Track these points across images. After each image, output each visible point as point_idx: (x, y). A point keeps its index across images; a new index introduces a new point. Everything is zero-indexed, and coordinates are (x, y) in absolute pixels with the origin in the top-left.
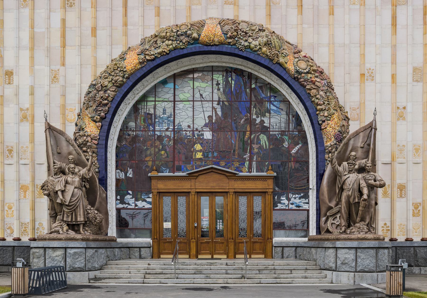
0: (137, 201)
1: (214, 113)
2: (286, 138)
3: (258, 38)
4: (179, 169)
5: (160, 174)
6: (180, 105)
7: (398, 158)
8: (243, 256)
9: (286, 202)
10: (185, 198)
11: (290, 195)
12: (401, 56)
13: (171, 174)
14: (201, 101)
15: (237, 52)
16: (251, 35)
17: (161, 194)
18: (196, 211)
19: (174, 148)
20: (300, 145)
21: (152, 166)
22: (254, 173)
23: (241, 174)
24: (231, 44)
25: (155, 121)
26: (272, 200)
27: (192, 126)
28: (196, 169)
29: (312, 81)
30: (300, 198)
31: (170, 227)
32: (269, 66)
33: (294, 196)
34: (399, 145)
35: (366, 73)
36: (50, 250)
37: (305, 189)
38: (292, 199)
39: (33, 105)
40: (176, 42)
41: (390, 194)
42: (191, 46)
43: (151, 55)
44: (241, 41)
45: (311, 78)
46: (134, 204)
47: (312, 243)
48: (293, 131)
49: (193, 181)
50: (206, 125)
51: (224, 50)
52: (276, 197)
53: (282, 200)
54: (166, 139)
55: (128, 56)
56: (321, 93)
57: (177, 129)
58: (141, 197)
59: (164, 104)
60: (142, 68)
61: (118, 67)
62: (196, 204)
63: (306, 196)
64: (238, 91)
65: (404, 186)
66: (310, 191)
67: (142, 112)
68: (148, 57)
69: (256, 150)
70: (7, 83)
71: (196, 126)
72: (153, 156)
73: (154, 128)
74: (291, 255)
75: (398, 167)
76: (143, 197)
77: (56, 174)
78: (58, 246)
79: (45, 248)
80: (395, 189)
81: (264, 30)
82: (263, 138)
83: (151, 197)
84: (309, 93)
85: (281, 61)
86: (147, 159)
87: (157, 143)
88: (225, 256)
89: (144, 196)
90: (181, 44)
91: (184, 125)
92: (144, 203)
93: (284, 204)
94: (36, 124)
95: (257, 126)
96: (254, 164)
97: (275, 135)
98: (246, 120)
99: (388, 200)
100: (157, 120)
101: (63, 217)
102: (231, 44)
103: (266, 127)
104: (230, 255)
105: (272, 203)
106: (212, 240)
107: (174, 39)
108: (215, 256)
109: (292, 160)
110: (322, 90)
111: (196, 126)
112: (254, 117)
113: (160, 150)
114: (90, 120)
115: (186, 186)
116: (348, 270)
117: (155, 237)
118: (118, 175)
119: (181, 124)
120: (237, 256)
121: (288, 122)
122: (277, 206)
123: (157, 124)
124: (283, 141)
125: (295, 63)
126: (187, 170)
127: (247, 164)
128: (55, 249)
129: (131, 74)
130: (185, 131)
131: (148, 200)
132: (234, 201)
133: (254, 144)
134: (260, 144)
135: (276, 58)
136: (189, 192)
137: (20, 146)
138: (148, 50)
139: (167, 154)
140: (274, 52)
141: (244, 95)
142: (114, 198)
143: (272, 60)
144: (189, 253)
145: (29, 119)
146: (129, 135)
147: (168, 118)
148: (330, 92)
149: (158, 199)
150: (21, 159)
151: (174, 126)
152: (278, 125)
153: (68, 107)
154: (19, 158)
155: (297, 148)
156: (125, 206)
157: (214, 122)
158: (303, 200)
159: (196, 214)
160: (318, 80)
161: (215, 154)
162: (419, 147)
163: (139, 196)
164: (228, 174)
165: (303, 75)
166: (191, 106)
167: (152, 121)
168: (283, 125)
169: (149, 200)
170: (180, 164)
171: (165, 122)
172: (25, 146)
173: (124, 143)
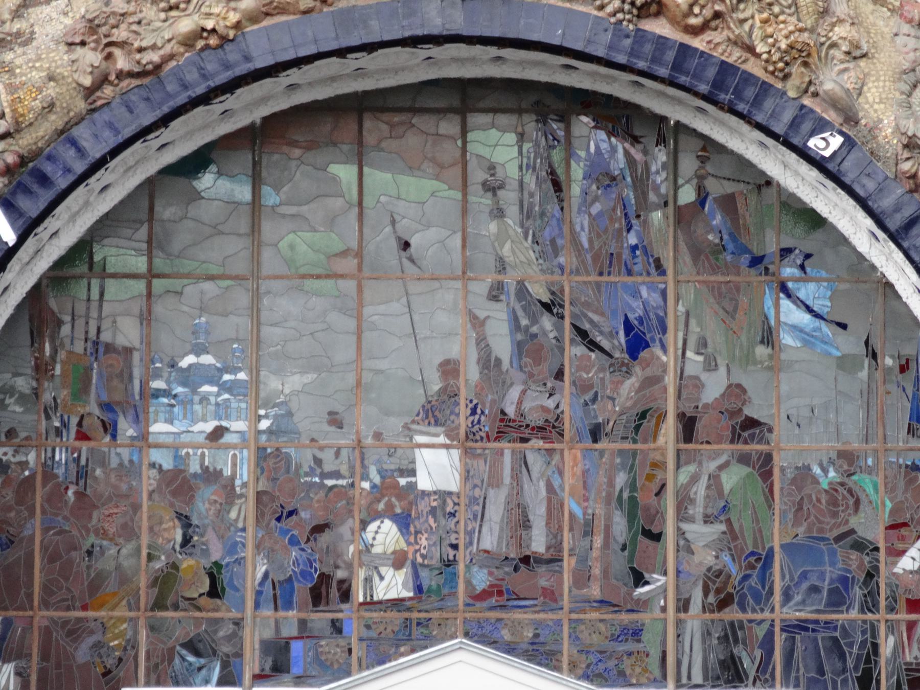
57: (269, 431)
171: (204, 399)
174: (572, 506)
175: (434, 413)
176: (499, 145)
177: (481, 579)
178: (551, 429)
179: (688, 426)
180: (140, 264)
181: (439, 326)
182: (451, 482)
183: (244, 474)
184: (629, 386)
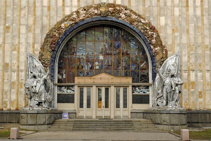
9: (138, 90)
20: (145, 63)
30: (145, 89)
35: (175, 29)
38: (141, 89)
46: (66, 91)
57: (87, 54)
74: (141, 117)
93: (138, 91)
155: (143, 64)
158: (146, 89)
174: (113, 61)
175: (101, 53)
176: (107, 30)
177: (105, 67)
178: (111, 54)
179: (123, 54)
180: (76, 40)
181: (101, 46)
182: (103, 59)
183: (85, 58)
184: (118, 51)
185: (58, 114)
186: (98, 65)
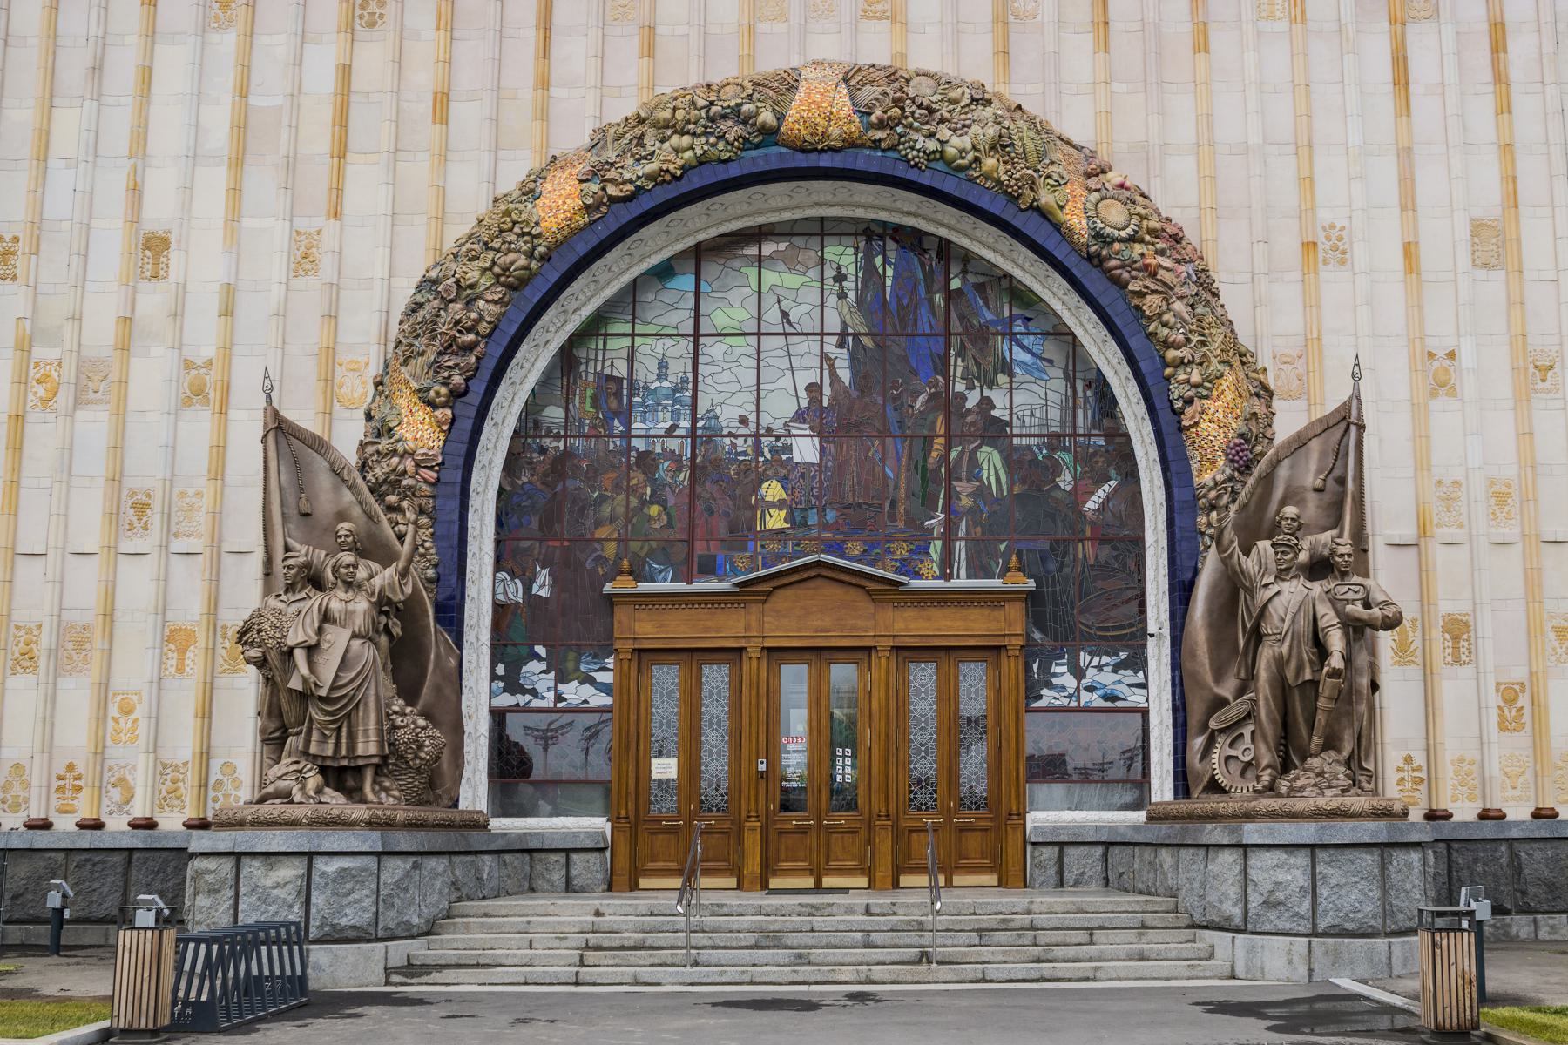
0: (563, 682)
1: (826, 373)
2: (1067, 457)
3: (969, 127)
4: (708, 568)
5: (644, 587)
6: (714, 349)
7: (1439, 525)
8: (923, 880)
9: (1070, 682)
10: (725, 669)
11: (1084, 658)
12: (1430, 183)
13: (681, 586)
14: (785, 334)
15: (900, 171)
16: (947, 115)
17: (646, 656)
18: (763, 717)
19: (693, 495)
20: (1113, 483)
21: (619, 558)
22: (962, 582)
23: (916, 584)
24: (884, 145)
25: (630, 401)
26: (1022, 676)
27: (752, 418)
28: (765, 566)
29: (1147, 266)
31: (674, 775)
32: (1007, 217)
33: (1096, 662)
34: (1440, 482)
36: (256, 863)
37: (1133, 636)
38: (1091, 672)
39: (227, 350)
40: (703, 139)
41: (1419, 652)
42: (753, 153)
43: (624, 182)
44: (915, 136)
45: (1142, 255)
46: (552, 694)
47: (1161, 831)
48: (1090, 435)
49: (754, 608)
50: (800, 416)
51: (860, 165)
52: (1035, 666)
53: (1055, 675)
54: (667, 464)
55: (548, 186)
56: (1178, 306)
57: (704, 428)
58: (578, 669)
59: (661, 345)
60: (591, 223)
61: (514, 223)
62: (763, 689)
63: (1137, 662)
64: (905, 302)
65: (1466, 624)
66: (1151, 642)
67: (589, 372)
68: (612, 190)
69: (966, 502)
70: (148, 274)
71: (766, 420)
72: (620, 522)
73: (628, 426)
74: (1089, 873)
75: (1440, 556)
76: (583, 668)
77: (290, 588)
78: (283, 849)
79: (238, 856)
80: (1437, 633)
81: (989, 102)
82: (991, 460)
83: (611, 666)
84: (1138, 308)
85: (1043, 201)
86: (602, 533)
87: (637, 477)
88: (862, 881)
89: (587, 663)
90: (721, 146)
91: (728, 417)
92: (587, 691)
93: (1064, 688)
94: (233, 414)
95: (969, 419)
96: (960, 546)
97: (1029, 447)
98: (931, 397)
99: (1414, 672)
100: (637, 399)
101: (308, 742)
102: (884, 145)
103: (998, 420)
104: (879, 875)
105: (1022, 687)
106: (819, 820)
107: (699, 130)
108: (828, 881)
109: (1088, 534)
110: (1180, 298)
111: (766, 420)
112: (960, 387)
113: (644, 503)
114: (415, 399)
115: (730, 627)
116: (1288, 926)
117: (623, 813)
118: (500, 590)
119: (718, 411)
120: (905, 880)
121: (1071, 406)
122: (1040, 697)
123: (636, 414)
124: (1056, 470)
125: (1090, 206)
126: (735, 571)
127: (936, 547)
128: (273, 859)
129: (558, 245)
130: (730, 435)
131: (601, 677)
132: (892, 680)
133: (959, 479)
134: (981, 480)
135: (1027, 191)
136: (741, 650)
137: (176, 490)
138: (612, 164)
139: (668, 515)
140: (1021, 170)
141: (924, 312)
142: (485, 672)
143: (1014, 198)
144: (737, 870)
145: (211, 396)
146: (543, 451)
147: (675, 391)
148: (1207, 304)
149: (633, 674)
150: (176, 535)
151: (694, 420)
152: (1038, 413)
153: (344, 357)
154: (170, 533)
156: (522, 699)
157: (825, 404)
158: (1128, 676)
159: (762, 729)
160: (1167, 263)
161: (831, 515)
162: (1509, 486)
163: (570, 665)
164: (872, 586)
165: (1117, 246)
166: (753, 351)
167: (620, 401)
168: (1055, 414)
169: (605, 678)
170: (713, 551)
171: (665, 407)
172: (191, 491)
173: (525, 479)
180: (627, 328)
185: (487, 858)
186: (780, 505)
